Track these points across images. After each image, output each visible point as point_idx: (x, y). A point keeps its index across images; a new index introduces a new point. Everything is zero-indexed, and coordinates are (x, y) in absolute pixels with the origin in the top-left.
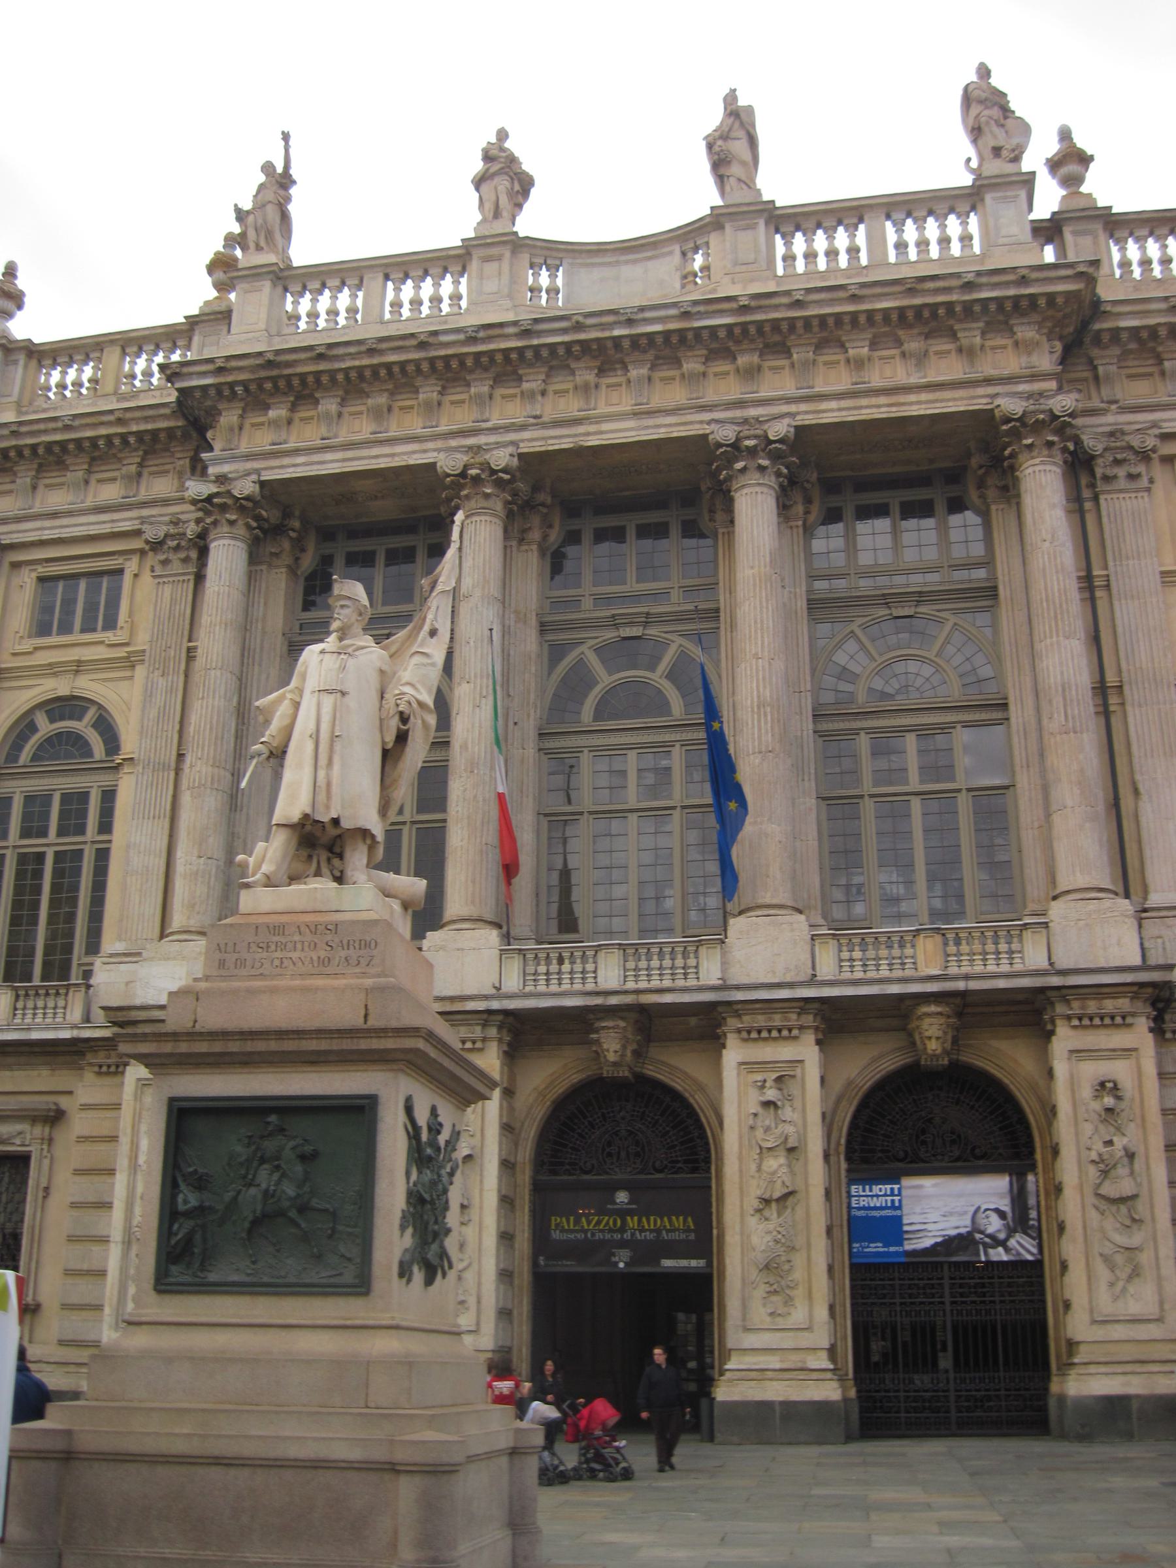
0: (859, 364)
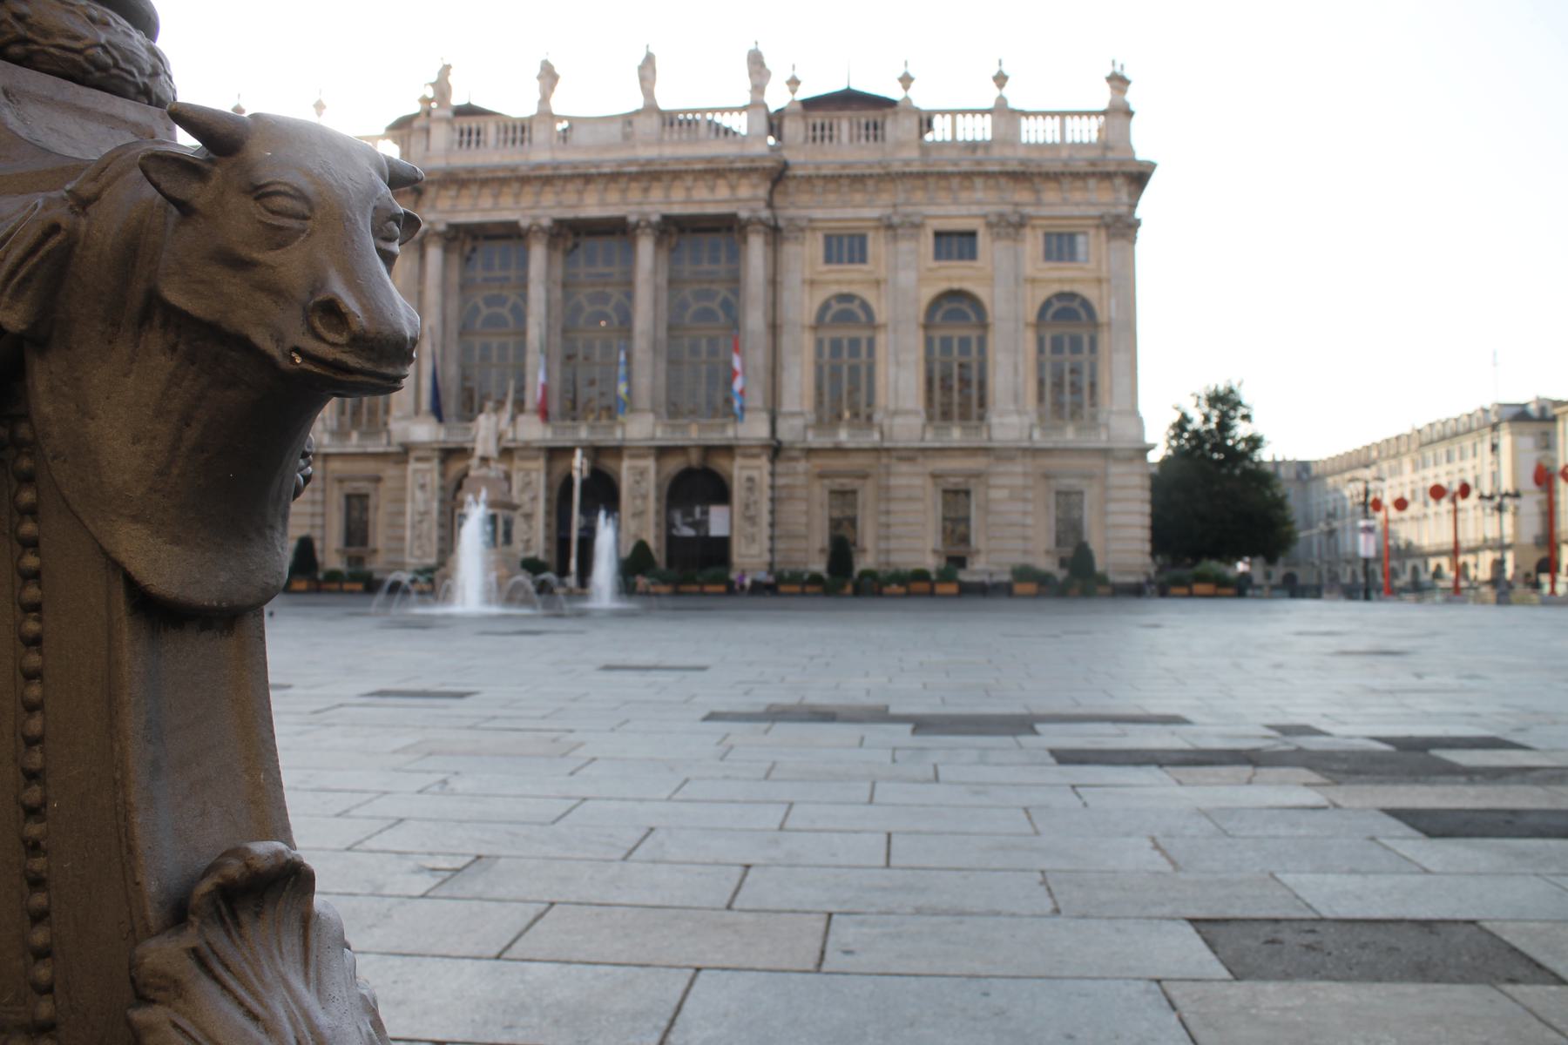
0: (688, 189)
